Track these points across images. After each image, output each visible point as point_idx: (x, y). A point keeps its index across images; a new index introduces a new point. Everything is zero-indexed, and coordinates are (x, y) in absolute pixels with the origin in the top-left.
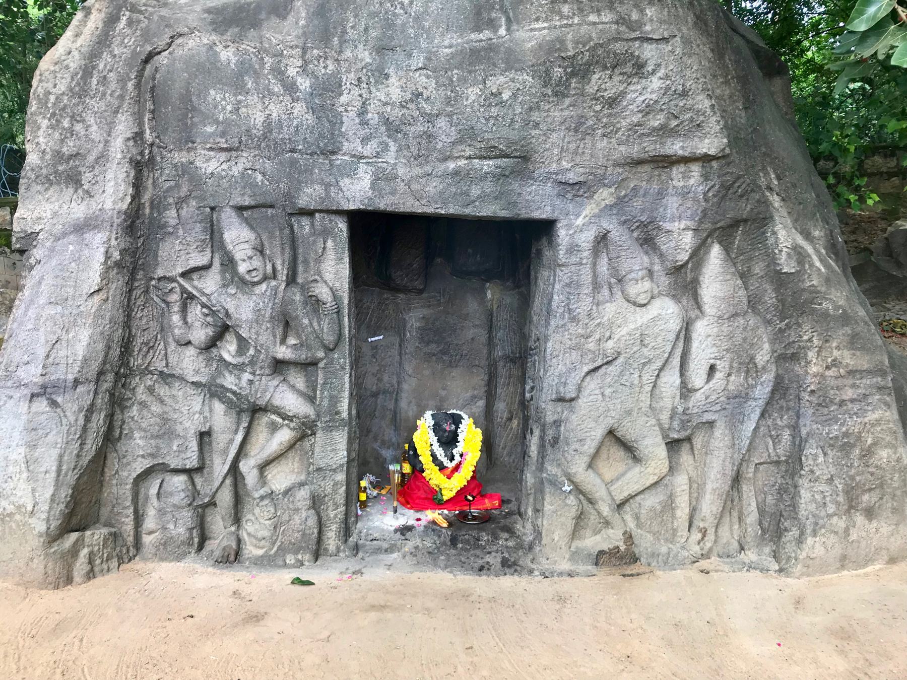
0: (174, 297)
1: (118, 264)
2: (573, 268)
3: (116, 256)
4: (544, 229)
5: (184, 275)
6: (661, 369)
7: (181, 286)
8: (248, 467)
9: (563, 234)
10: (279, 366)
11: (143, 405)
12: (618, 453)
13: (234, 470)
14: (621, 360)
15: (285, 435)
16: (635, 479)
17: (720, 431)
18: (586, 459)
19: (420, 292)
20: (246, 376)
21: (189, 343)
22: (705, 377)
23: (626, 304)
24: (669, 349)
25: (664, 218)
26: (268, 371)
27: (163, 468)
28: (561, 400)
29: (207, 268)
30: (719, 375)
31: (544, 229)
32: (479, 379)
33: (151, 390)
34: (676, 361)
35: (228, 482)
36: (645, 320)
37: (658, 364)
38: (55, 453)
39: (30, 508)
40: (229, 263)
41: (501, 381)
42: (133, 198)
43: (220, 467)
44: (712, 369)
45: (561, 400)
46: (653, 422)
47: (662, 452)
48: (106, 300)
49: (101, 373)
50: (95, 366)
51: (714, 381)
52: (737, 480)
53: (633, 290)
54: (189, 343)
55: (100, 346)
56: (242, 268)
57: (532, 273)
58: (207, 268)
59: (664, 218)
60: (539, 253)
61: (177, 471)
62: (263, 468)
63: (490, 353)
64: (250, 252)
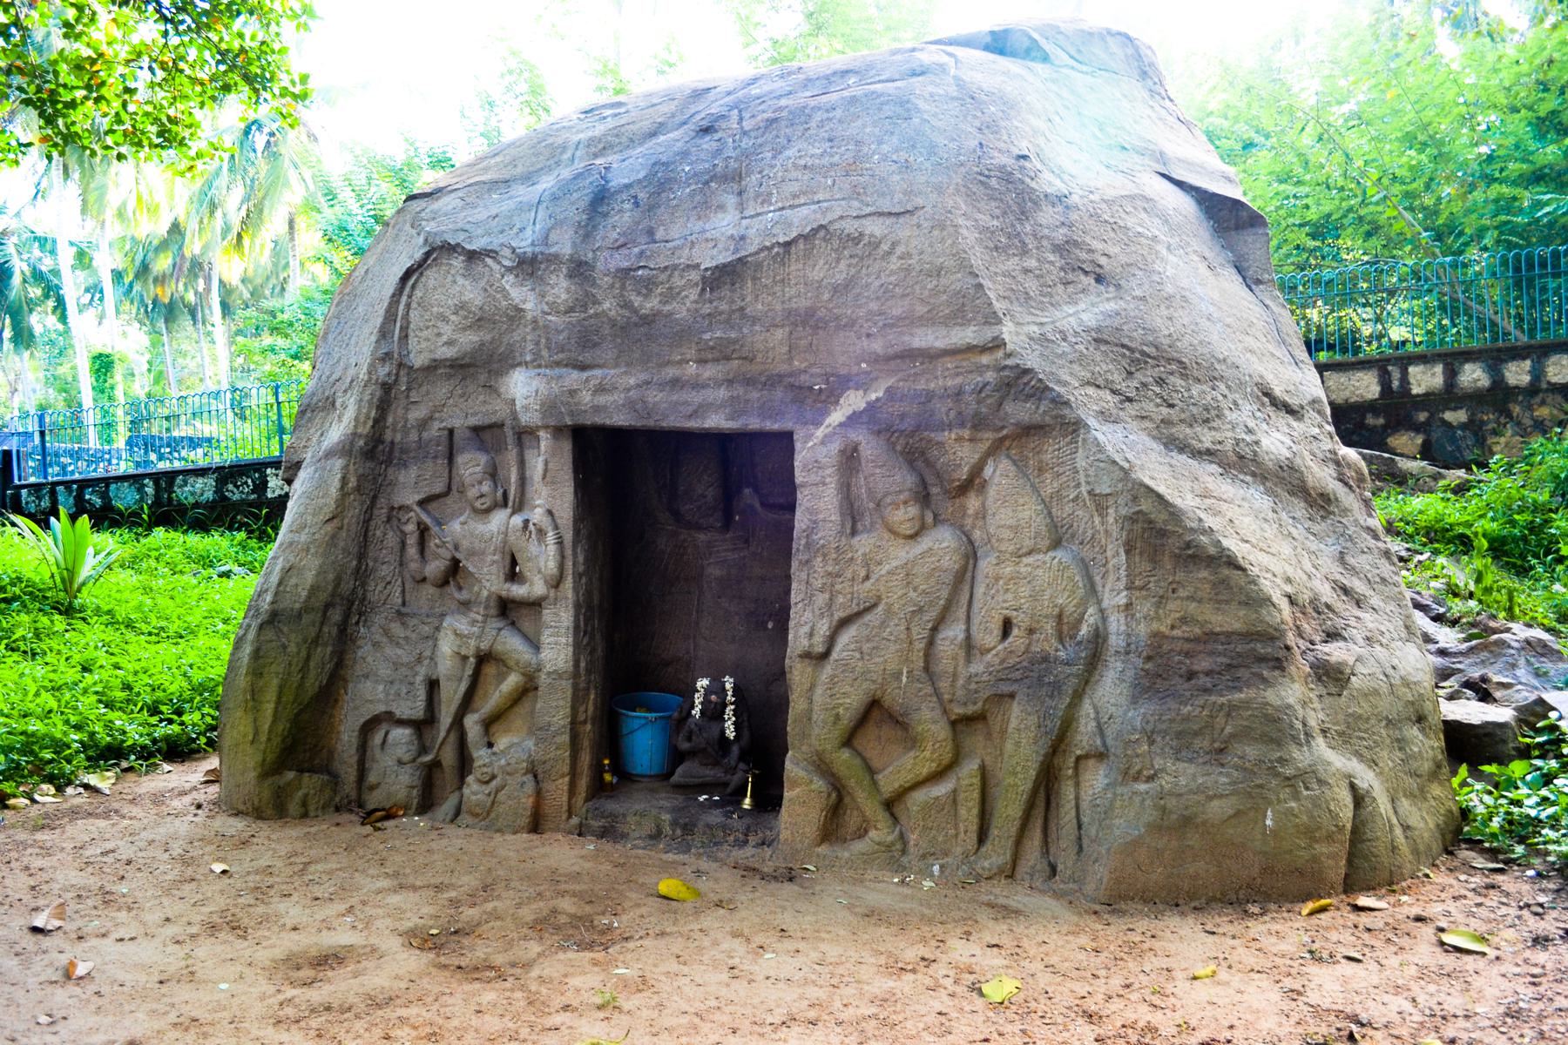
0: (410, 528)
2: (814, 489)
8: (472, 722)
10: (506, 609)
11: (376, 645)
14: (880, 608)
21: (424, 580)
22: (997, 631)
23: (886, 535)
24: (945, 593)
27: (388, 718)
30: (1015, 631)
36: (911, 556)
37: (932, 614)
42: (376, 421)
43: (445, 719)
46: (929, 690)
47: (941, 731)
48: (341, 528)
49: (328, 606)
50: (323, 597)
51: (1010, 639)
54: (424, 580)
55: (331, 576)
61: (401, 722)
62: (489, 724)
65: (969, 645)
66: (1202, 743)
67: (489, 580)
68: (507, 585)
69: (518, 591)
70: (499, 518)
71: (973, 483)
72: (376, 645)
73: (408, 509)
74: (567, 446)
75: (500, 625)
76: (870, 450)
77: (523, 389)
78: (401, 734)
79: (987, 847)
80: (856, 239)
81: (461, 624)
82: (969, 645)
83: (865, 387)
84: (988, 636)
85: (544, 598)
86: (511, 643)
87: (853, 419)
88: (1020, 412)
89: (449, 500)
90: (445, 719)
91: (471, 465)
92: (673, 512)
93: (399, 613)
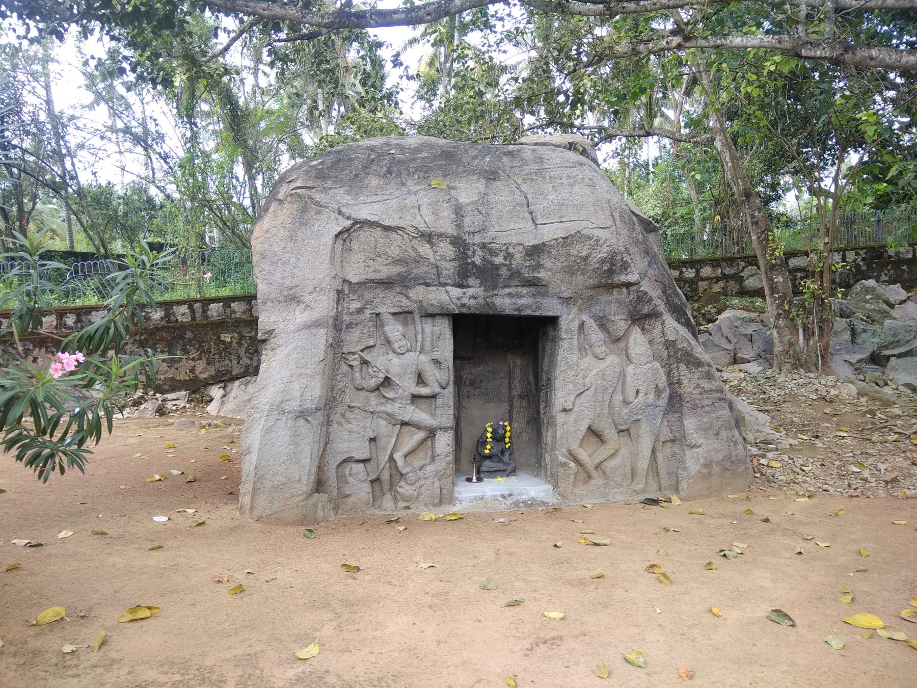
0: (355, 363)
1: (331, 345)
3: (331, 340)
4: (553, 321)
5: (362, 351)
6: (613, 393)
7: (361, 357)
9: (563, 324)
10: (415, 398)
12: (593, 439)
13: (391, 459)
14: (592, 388)
15: (421, 435)
16: (603, 452)
17: (643, 425)
18: (579, 442)
19: (469, 359)
20: (397, 405)
24: (615, 381)
25: (610, 315)
26: (409, 402)
28: (565, 410)
29: (373, 346)
30: (641, 395)
31: (553, 321)
32: (505, 407)
33: (343, 416)
34: (619, 388)
35: (388, 465)
37: (611, 390)
38: (309, 447)
39: (297, 478)
41: (515, 410)
44: (638, 391)
45: (565, 410)
50: (323, 401)
52: (654, 452)
53: (598, 351)
56: (396, 346)
57: (540, 345)
58: (373, 346)
59: (610, 315)
60: (546, 334)
63: (510, 393)
64: (400, 337)
65: (626, 402)
66: (710, 432)
68: (417, 389)
69: (424, 391)
72: (340, 424)
73: (353, 353)
75: (413, 408)
79: (635, 481)
82: (626, 402)
84: (631, 398)
85: (439, 394)
88: (646, 309)
89: (375, 349)
91: (394, 329)
93: (349, 407)
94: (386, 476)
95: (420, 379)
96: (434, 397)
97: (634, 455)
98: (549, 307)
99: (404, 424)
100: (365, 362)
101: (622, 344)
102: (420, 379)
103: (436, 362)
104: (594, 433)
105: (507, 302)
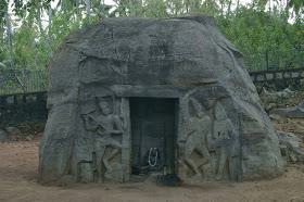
4: (178, 99)
10: (113, 135)
15: (116, 151)
40: (101, 110)
43: (99, 160)
67: (110, 130)
69: (117, 132)
70: (110, 117)
71: (213, 107)
74: (128, 102)
76: (195, 101)
77: (117, 89)
78: (88, 165)
80: (191, 62)
81: (102, 139)
83: (191, 89)
86: (115, 142)
87: (193, 95)
88: (223, 94)
90: (99, 160)
91: (104, 105)
92: (155, 114)
94: (99, 170)
95: (115, 127)
96: (120, 134)
97: (218, 163)
98: (173, 94)
99: (107, 146)
100: (90, 119)
101: (211, 111)
102: (115, 127)
103: (122, 119)
104: (198, 152)
105: (156, 91)
